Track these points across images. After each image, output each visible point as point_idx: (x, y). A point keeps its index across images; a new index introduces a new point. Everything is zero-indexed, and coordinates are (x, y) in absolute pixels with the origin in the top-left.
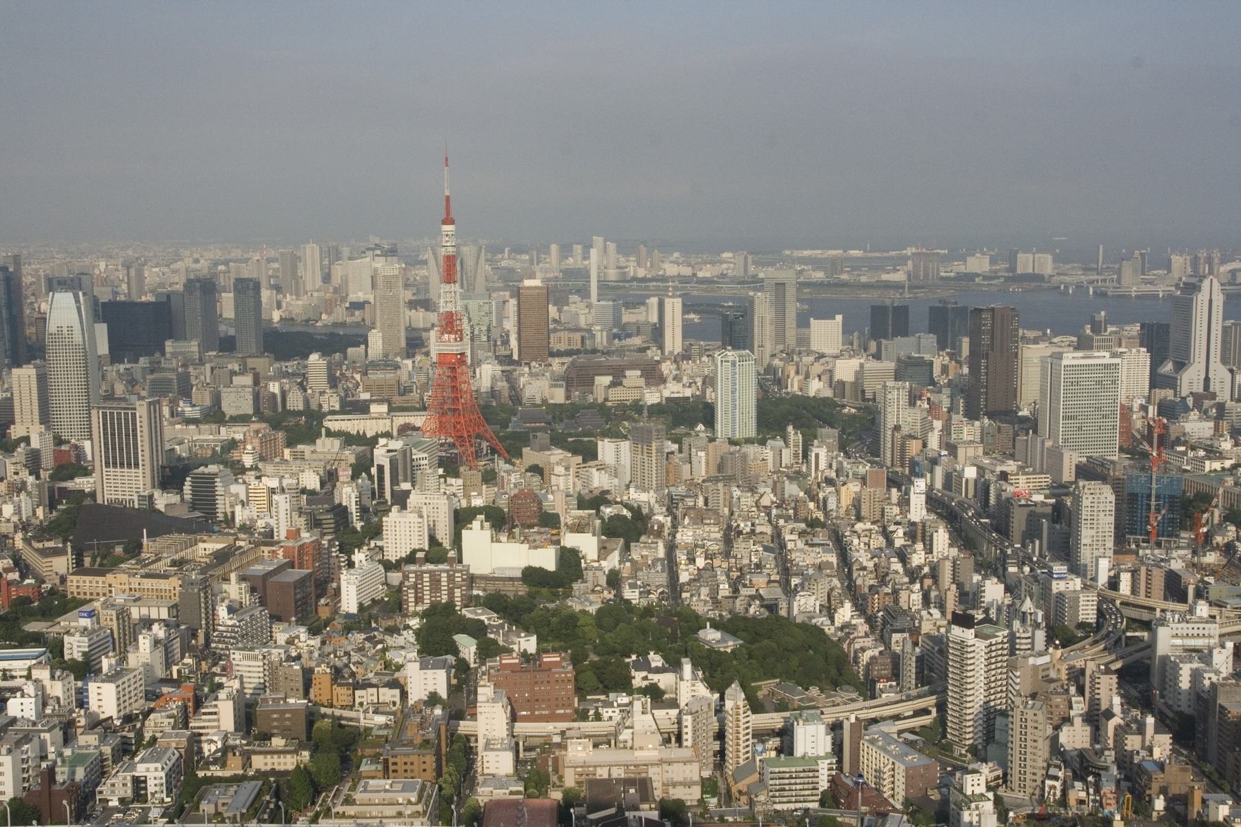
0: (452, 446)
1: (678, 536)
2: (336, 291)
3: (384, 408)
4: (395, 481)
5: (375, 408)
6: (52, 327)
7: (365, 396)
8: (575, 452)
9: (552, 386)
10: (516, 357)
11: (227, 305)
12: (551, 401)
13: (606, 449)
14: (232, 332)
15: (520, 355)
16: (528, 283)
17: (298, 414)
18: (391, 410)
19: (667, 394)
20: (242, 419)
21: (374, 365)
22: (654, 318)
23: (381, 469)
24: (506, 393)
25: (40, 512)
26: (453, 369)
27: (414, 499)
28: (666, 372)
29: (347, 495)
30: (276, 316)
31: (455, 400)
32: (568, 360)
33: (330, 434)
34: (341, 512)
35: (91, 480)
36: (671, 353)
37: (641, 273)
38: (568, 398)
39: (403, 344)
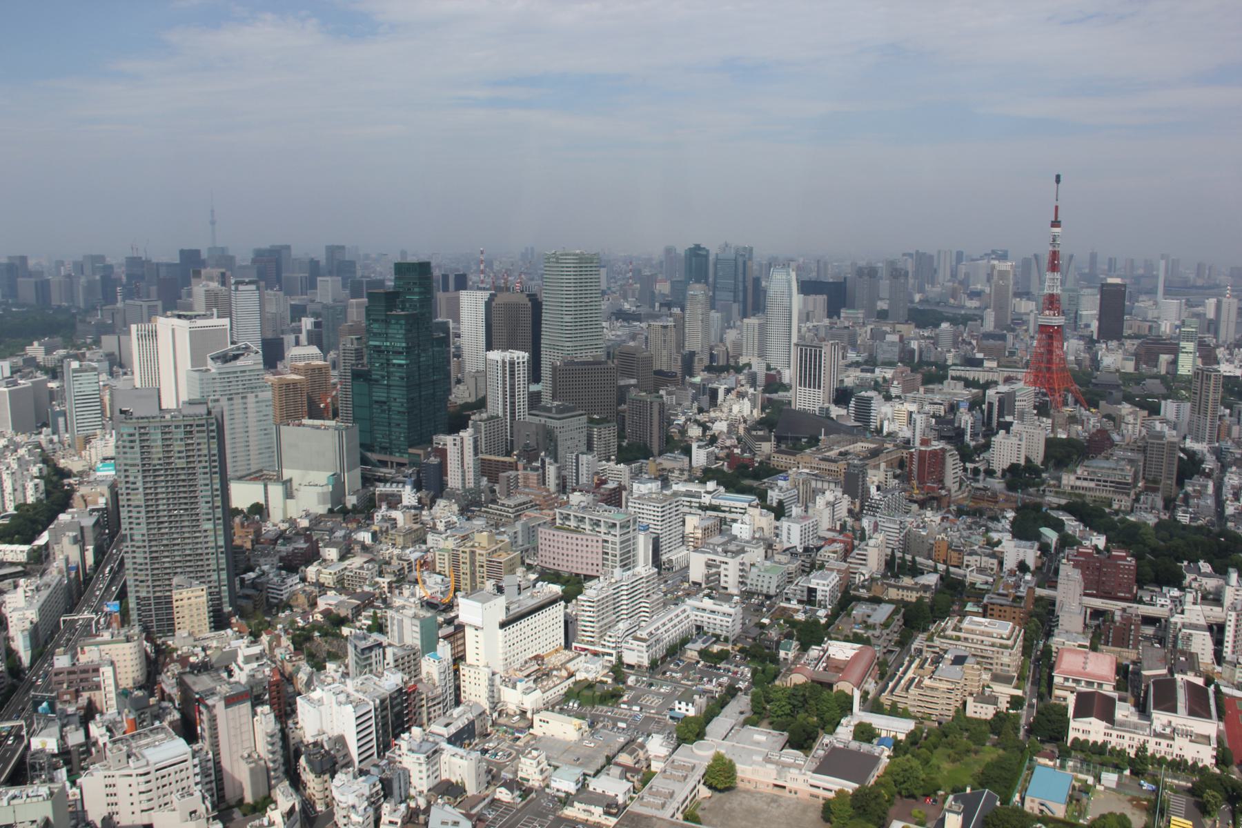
0: (1045, 395)
1: (1226, 479)
2: (961, 283)
3: (994, 364)
4: (1001, 414)
5: (987, 364)
6: (771, 293)
7: (980, 356)
8: (1142, 407)
9: (1124, 359)
10: (1095, 337)
11: (884, 284)
13: (1169, 408)
14: (885, 307)
16: (1110, 280)
17: (929, 364)
18: (999, 366)
20: (889, 364)
21: (988, 336)
22: (1211, 315)
23: (991, 404)
24: (1087, 363)
25: (755, 412)
26: (1050, 337)
27: (1015, 427)
28: (1219, 356)
29: (966, 419)
30: (917, 297)
31: (1050, 361)
32: (1136, 342)
33: (953, 378)
34: (960, 433)
35: (788, 394)
37: (1200, 282)
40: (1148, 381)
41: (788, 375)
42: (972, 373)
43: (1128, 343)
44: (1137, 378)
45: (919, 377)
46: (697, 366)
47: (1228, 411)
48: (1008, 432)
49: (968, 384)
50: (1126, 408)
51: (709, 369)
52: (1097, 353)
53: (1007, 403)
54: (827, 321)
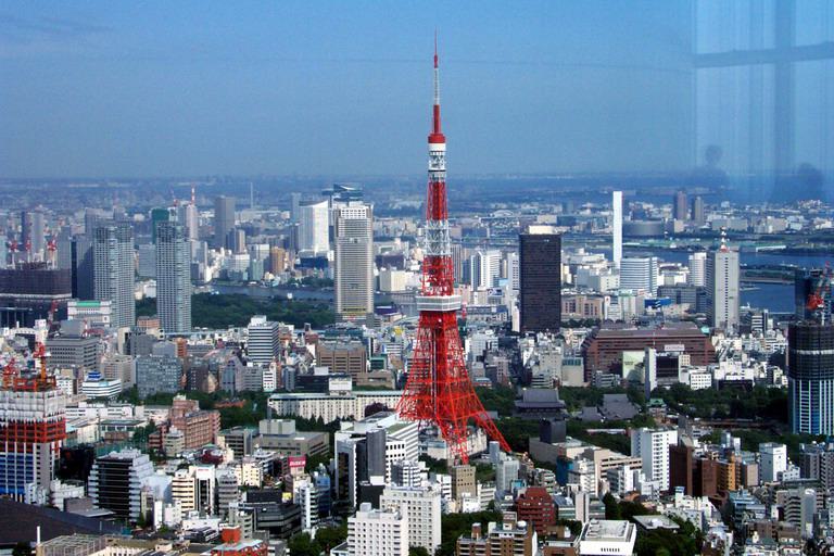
3: (347, 385)
5: (335, 386)
7: (322, 371)
10: (516, 328)
12: (565, 384)
15: (521, 326)
16: (534, 230)
18: (353, 390)
19: (719, 375)
22: (700, 281)
23: (345, 458)
24: (506, 372)
26: (439, 333)
27: (386, 497)
29: (303, 486)
31: (441, 374)
34: (294, 510)
36: (725, 324)
38: (587, 376)
39: (370, 309)
40: (607, 397)
42: (310, 406)
43: (569, 333)
44: (591, 395)
45: (216, 415)
47: (737, 441)
48: (376, 505)
49: (304, 425)
50: (573, 449)
52: (519, 354)
53: (369, 451)
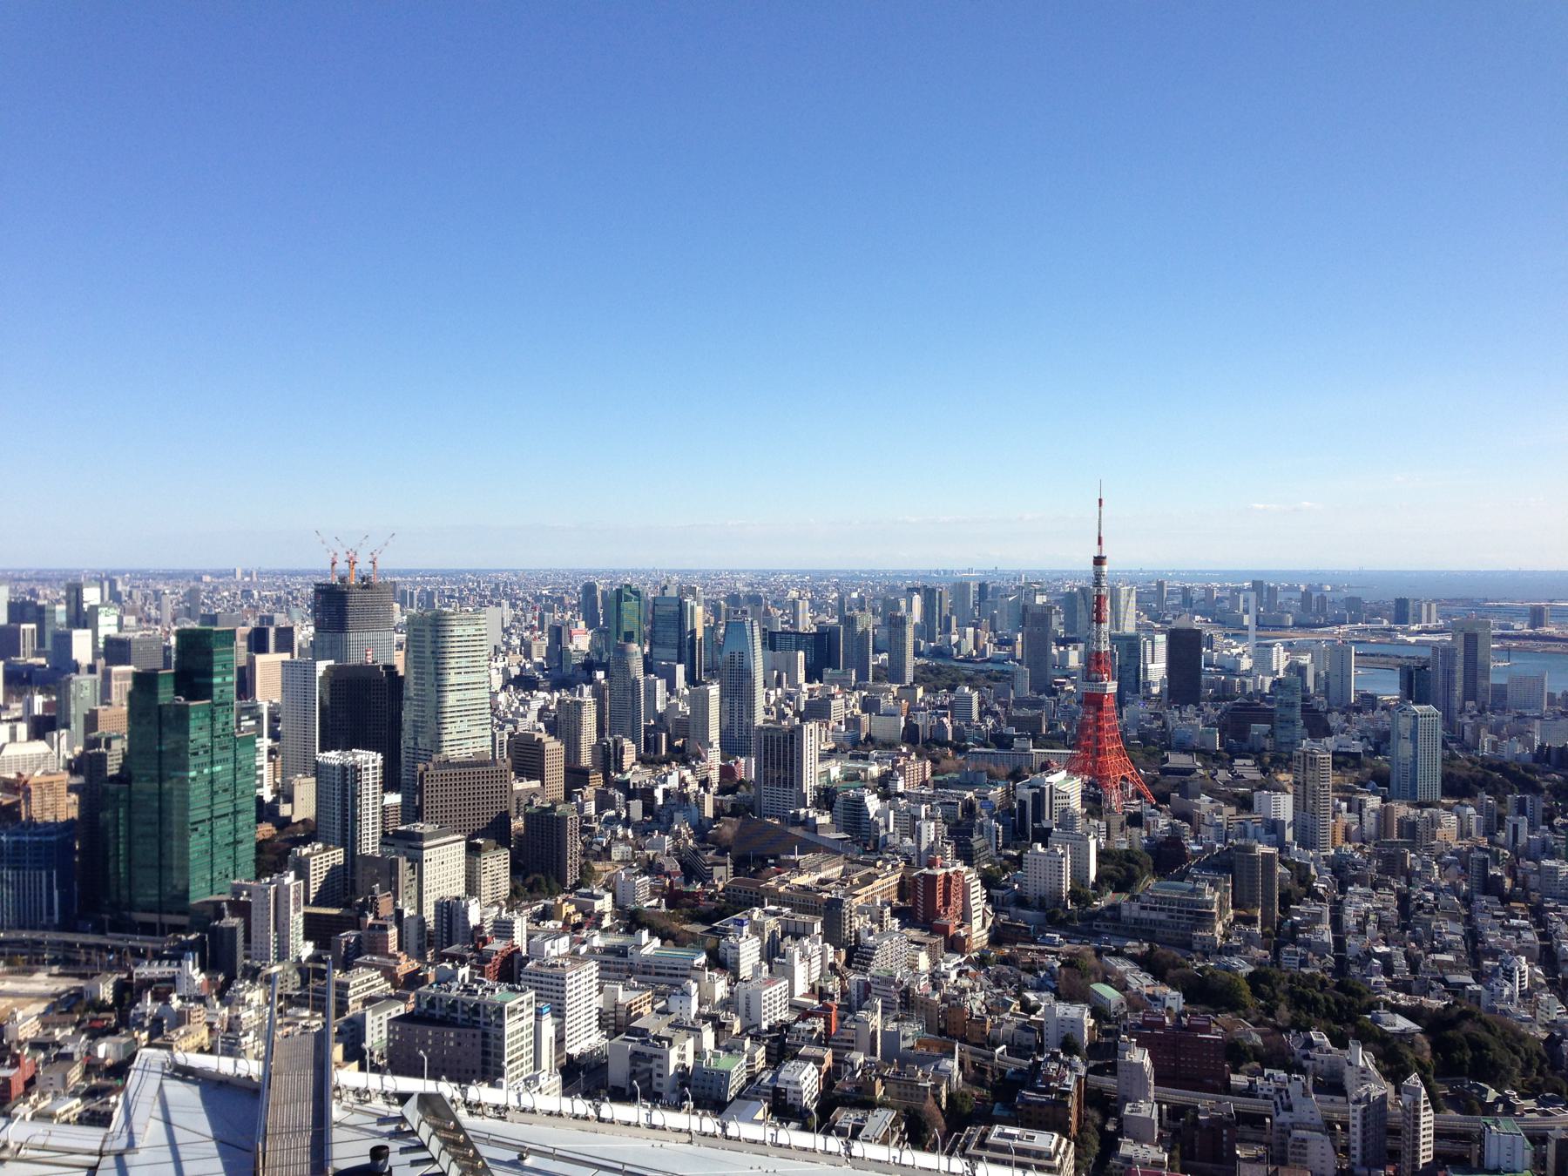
7: (1012, 731)
21: (1020, 703)
41: (747, 767)
46: (629, 758)
51: (641, 760)
54: (805, 687)
